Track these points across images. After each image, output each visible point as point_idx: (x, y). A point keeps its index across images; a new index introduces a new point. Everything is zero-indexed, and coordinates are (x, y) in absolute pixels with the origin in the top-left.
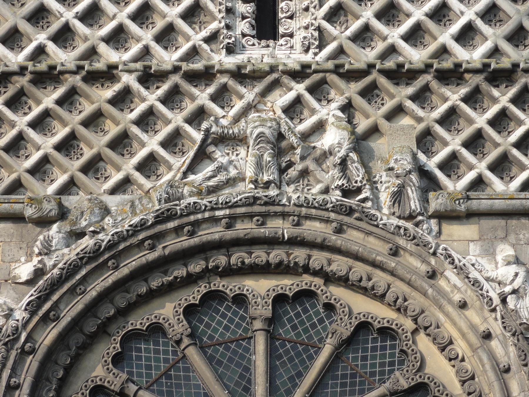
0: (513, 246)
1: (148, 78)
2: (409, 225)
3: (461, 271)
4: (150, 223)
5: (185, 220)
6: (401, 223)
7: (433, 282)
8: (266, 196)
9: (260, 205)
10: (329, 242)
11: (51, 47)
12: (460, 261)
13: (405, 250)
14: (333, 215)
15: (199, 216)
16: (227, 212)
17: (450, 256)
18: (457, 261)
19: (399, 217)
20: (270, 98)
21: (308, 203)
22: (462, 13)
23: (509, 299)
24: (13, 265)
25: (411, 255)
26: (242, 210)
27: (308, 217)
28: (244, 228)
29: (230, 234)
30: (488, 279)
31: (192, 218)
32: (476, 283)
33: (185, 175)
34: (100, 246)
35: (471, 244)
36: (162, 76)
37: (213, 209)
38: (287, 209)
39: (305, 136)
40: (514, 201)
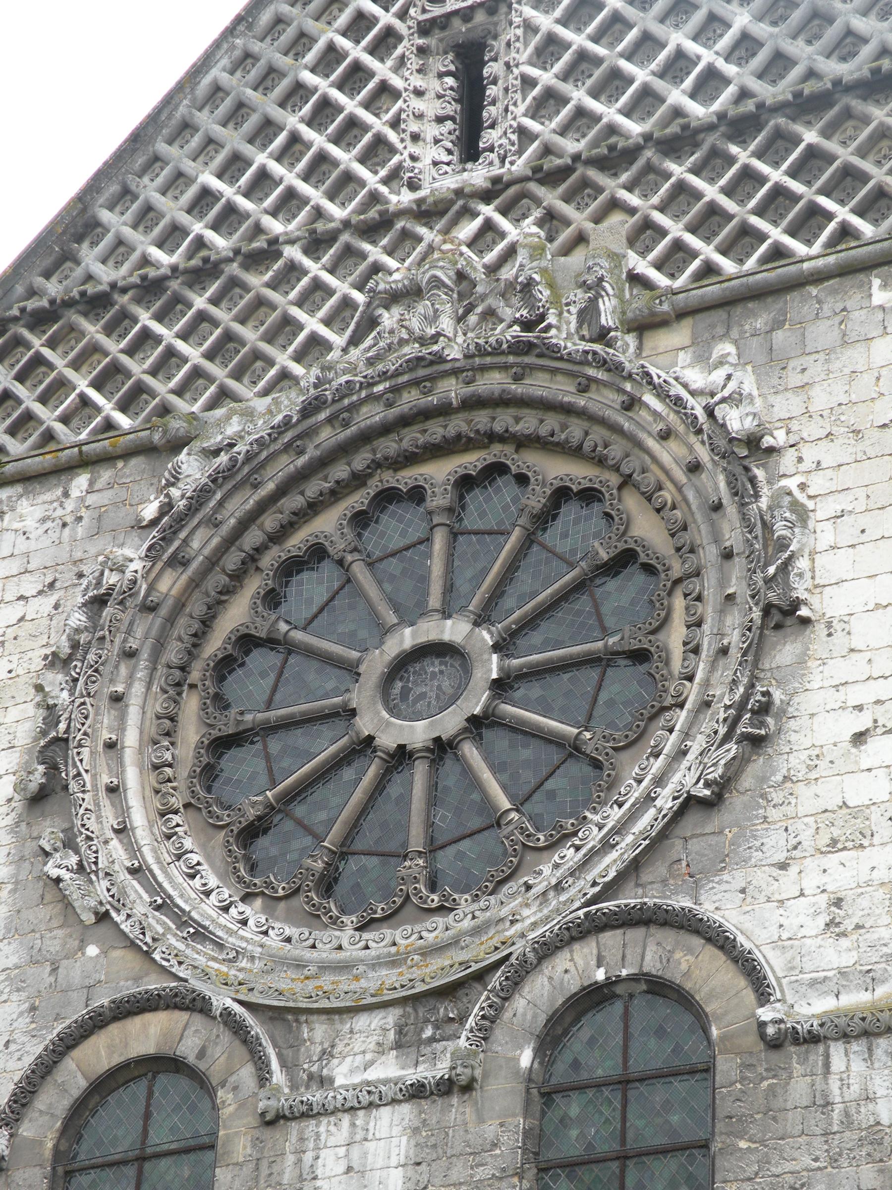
0: (735, 342)
1: (315, 245)
2: (597, 347)
3: (661, 392)
5: (338, 406)
6: (588, 346)
7: (630, 414)
8: (430, 354)
9: (424, 367)
10: (509, 393)
11: (211, 236)
12: (659, 377)
14: (511, 359)
15: (355, 398)
16: (387, 384)
17: (648, 374)
19: (592, 340)
21: (480, 351)
22: (699, 58)
23: (718, 413)
24: (140, 507)
25: (605, 386)
26: (405, 378)
27: (483, 369)
29: (393, 412)
31: (346, 402)
32: (678, 401)
33: (345, 350)
34: (236, 461)
35: (681, 354)
36: (331, 238)
37: (371, 385)
38: (458, 364)
39: (492, 270)
40: (733, 282)
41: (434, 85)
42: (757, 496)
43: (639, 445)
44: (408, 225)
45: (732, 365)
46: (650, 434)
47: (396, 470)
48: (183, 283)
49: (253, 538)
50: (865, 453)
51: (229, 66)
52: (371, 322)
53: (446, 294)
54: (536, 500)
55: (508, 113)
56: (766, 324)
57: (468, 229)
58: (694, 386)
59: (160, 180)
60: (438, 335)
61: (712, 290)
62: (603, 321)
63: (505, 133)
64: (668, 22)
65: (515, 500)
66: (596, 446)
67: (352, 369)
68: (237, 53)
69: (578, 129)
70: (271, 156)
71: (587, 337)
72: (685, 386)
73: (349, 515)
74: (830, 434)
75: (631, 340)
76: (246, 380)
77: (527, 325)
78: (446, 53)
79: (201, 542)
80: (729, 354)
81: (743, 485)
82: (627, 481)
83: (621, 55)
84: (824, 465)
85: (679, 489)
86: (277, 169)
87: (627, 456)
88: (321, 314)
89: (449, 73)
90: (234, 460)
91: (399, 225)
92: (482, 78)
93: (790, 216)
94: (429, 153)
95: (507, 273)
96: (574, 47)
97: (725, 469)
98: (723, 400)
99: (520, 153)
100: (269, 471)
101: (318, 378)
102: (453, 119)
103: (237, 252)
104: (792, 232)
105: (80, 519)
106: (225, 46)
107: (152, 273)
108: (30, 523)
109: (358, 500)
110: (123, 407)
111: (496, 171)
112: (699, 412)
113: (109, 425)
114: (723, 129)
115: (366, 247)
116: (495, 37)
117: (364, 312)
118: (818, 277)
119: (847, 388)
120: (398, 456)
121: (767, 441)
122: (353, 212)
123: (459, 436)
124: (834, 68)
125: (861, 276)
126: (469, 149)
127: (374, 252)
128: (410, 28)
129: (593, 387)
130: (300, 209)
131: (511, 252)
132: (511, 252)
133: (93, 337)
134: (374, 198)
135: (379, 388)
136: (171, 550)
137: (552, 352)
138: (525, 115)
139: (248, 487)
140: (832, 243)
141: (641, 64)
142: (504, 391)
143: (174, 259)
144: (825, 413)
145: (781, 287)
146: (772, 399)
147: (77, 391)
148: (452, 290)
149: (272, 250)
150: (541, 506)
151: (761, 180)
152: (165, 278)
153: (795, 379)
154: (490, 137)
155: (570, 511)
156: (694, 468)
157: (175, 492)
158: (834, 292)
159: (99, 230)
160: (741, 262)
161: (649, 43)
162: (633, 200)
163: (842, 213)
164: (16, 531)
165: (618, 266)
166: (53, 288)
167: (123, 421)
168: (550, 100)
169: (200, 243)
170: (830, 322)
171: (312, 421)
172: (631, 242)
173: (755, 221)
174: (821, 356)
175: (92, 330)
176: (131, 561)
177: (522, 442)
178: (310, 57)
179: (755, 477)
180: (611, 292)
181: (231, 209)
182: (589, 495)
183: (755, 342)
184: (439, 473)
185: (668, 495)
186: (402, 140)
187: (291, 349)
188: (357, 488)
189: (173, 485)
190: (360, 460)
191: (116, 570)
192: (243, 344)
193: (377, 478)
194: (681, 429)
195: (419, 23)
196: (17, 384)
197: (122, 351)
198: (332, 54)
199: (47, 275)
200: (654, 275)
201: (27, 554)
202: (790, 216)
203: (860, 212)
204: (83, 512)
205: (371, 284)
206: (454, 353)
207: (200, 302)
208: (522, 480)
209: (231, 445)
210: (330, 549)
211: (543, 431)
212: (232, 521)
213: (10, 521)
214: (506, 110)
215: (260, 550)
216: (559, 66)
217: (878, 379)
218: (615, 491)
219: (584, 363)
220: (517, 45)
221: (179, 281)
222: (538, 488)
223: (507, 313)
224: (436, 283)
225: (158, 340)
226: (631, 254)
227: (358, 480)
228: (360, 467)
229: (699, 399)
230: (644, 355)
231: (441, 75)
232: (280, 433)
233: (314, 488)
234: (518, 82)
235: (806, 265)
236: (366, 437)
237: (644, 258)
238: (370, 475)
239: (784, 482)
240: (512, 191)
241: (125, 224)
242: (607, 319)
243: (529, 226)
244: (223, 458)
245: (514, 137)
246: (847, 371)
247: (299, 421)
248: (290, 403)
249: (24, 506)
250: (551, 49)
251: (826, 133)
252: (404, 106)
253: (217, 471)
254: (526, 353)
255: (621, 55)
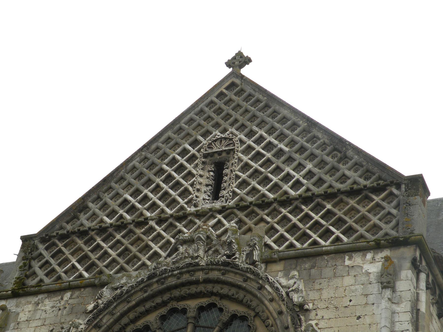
0: (298, 271)
1: (160, 222)
2: (251, 267)
4: (145, 280)
5: (161, 277)
7: (260, 291)
9: (192, 267)
10: (220, 279)
11: (125, 215)
13: (250, 278)
14: (222, 267)
15: (167, 275)
17: (268, 278)
18: (270, 280)
19: (250, 264)
20: (207, 223)
22: (294, 176)
25: (253, 280)
26: (185, 270)
27: (212, 270)
28: (186, 277)
29: (180, 281)
30: (283, 287)
31: (164, 276)
32: (277, 289)
33: (166, 258)
34: (123, 292)
35: (280, 273)
36: (166, 220)
37: (173, 271)
38: (203, 267)
39: (219, 236)
40: (299, 251)
41: (207, 174)
42: (301, 326)
43: (262, 303)
44: (192, 219)
45: (296, 279)
46: (266, 299)
47: (178, 302)
48: (113, 230)
49: (125, 320)
50: (339, 315)
51: (139, 161)
52: (175, 249)
53: (202, 243)
54: (225, 318)
55: (230, 186)
56: (309, 266)
57: (212, 222)
58: (283, 284)
59: (111, 195)
60: (198, 256)
61: (292, 252)
62: (254, 258)
63: (228, 192)
64: (285, 164)
65: (218, 317)
66: (248, 301)
67: (167, 265)
68: (143, 157)
69: (253, 194)
70: (149, 191)
71: (249, 263)
72: (280, 284)
73: (160, 316)
74: (327, 307)
75: (263, 266)
76: (130, 265)
77: (229, 257)
78: (211, 164)
79: (107, 320)
80: (296, 275)
81: (297, 321)
82: (257, 315)
83: (269, 172)
84: (325, 318)
85: (275, 320)
86: (151, 195)
87: (258, 306)
88: (159, 245)
89: (211, 171)
90: (122, 292)
91: (189, 218)
92: (222, 174)
93: (320, 231)
94: (202, 196)
95: (224, 238)
96: (254, 168)
97: (291, 315)
98: (292, 290)
99: (232, 199)
100: (134, 297)
101: (155, 266)
102: (211, 186)
103: (133, 221)
104: (320, 237)
105: (65, 308)
106: (139, 154)
107: (103, 225)
108: (48, 308)
109: (163, 311)
110: (87, 270)
111: (224, 204)
112: (284, 293)
113: (81, 276)
114: (300, 200)
115: (178, 224)
116: (228, 161)
117: (174, 246)
118: (328, 253)
119: (334, 292)
120: (179, 297)
121: (306, 307)
122: (174, 212)
123: (201, 292)
124: (338, 186)
125: (342, 255)
126: (216, 196)
127: (180, 226)
128: (201, 155)
129: (249, 280)
130: (157, 209)
131: (226, 231)
132: (226, 231)
133: (80, 245)
134: (182, 208)
135: (176, 272)
136: (95, 322)
137: (236, 266)
138: (235, 187)
139: (126, 302)
140: (333, 242)
141: (275, 176)
142: (218, 278)
143: (111, 221)
144: (326, 300)
145: (315, 254)
146: (309, 292)
147: (72, 263)
148: (205, 242)
149: (146, 221)
150: (226, 320)
151: (312, 218)
152: (107, 227)
153: (317, 287)
154: (223, 193)
155: (236, 323)
156: (280, 313)
157: (100, 302)
158: (332, 258)
159: (88, 209)
160: (302, 244)
161: (278, 170)
162: (269, 219)
163: (337, 233)
164: (42, 310)
165: (261, 240)
166: (69, 227)
167: (86, 275)
168: (243, 184)
169: (121, 217)
170: (330, 269)
171: (151, 281)
172: (267, 233)
173: (308, 231)
174: (327, 280)
175: (80, 243)
176: (81, 324)
177: (223, 297)
178: (166, 161)
179: (301, 319)
180: (258, 249)
181: (133, 207)
182: (243, 318)
183: (305, 272)
184: (193, 304)
185: (270, 321)
186: (194, 191)
187: (147, 256)
188: (164, 306)
189: (100, 299)
190: (166, 297)
191: (75, 327)
192: (131, 252)
193: (171, 304)
194: (277, 299)
195: (204, 154)
196: (51, 258)
197: (89, 251)
198: (174, 161)
199: (68, 223)
200: (273, 245)
201: (45, 319)
202: (320, 231)
203: (344, 233)
204: (67, 306)
205: (177, 237)
206: (203, 263)
207: (118, 237)
208: (221, 310)
209: (122, 287)
210: (151, 327)
211: (230, 294)
212: (119, 314)
213: (41, 306)
214: (229, 185)
215: (127, 325)
216: (248, 173)
217: (345, 290)
218: (252, 318)
219: (247, 272)
220: (235, 165)
221: (112, 229)
222: (226, 313)
223: (222, 252)
224: (200, 239)
225: (102, 248)
226: (266, 237)
227: (164, 304)
228: (165, 299)
229: (284, 289)
230: (267, 271)
231: (209, 171)
232: (139, 284)
233: (148, 305)
234: (234, 177)
235: (324, 248)
236: (169, 289)
237: (270, 239)
238: (169, 302)
239: (310, 322)
240: (228, 211)
241: (97, 208)
242: (256, 258)
243: (233, 223)
244: (119, 291)
245: (231, 194)
246: (335, 286)
247: (146, 281)
248: (144, 274)
249: (47, 302)
250: (246, 167)
251: (334, 206)
252: (196, 180)
253: (116, 295)
254: (227, 266)
255: (269, 172)
